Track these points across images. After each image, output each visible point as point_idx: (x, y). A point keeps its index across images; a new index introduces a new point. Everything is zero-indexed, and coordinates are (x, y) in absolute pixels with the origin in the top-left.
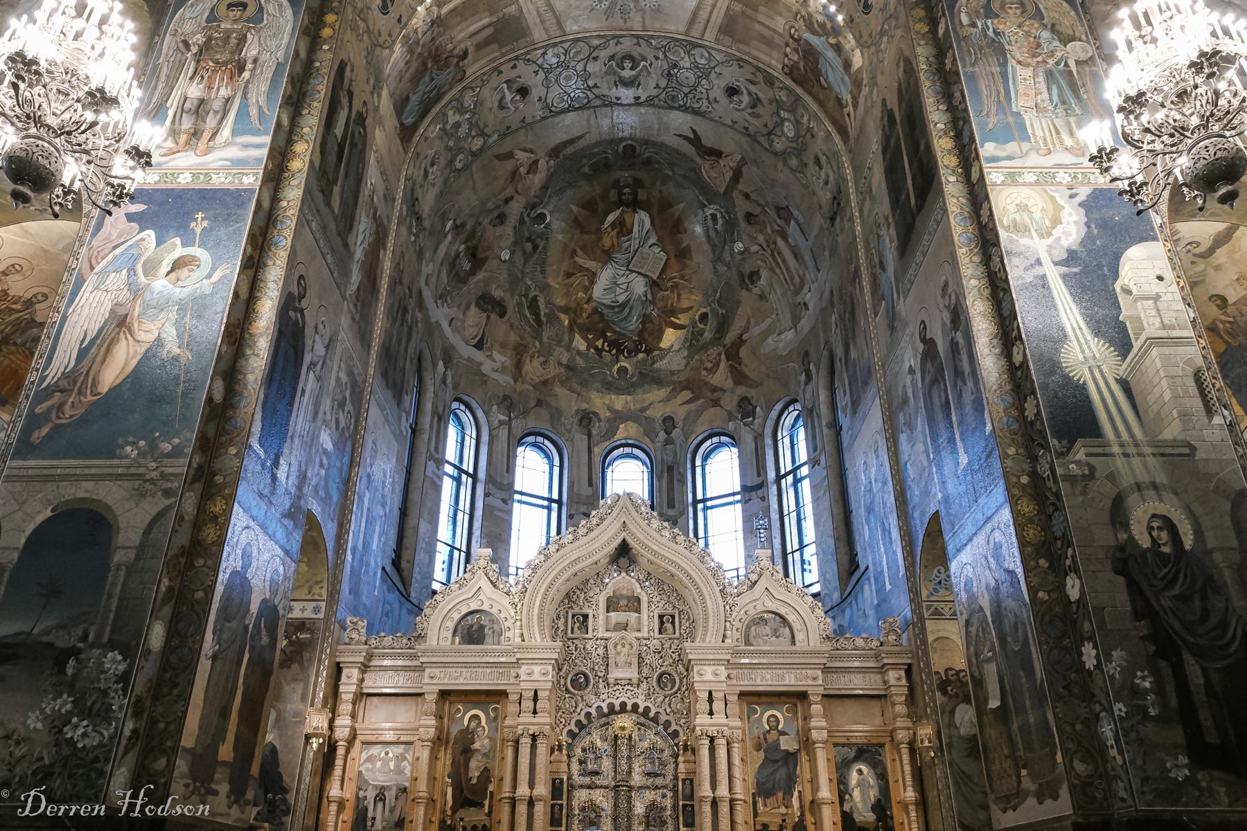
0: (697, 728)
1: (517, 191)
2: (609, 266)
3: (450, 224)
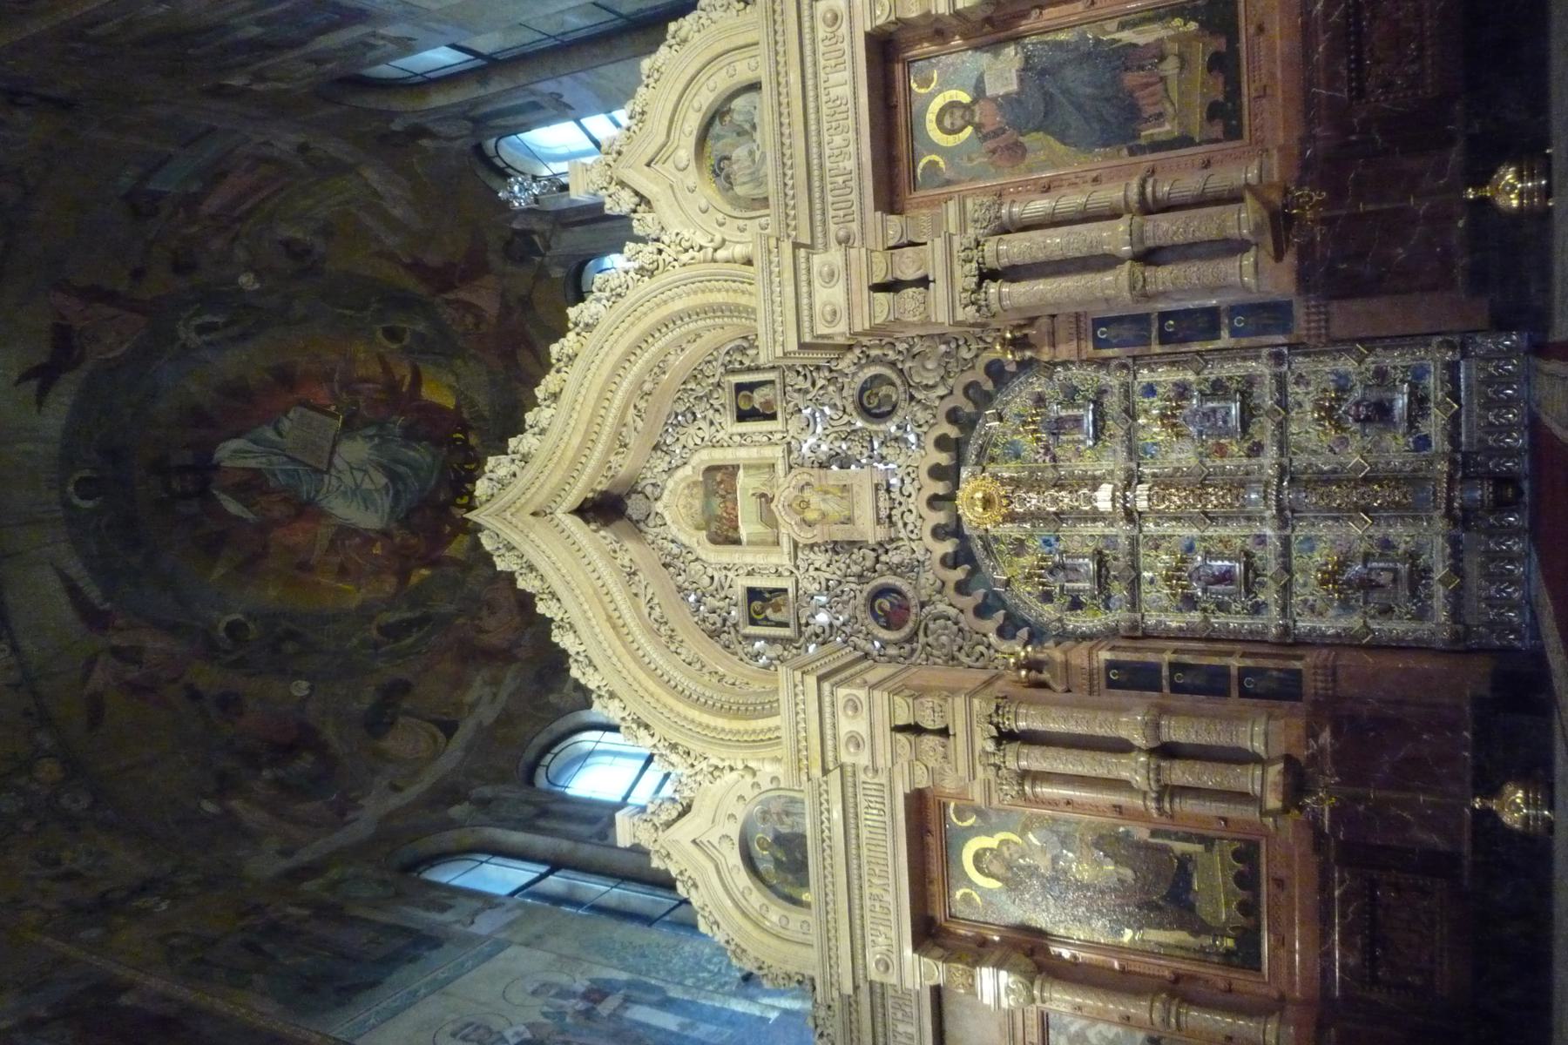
0: (960, 316)
1: (174, 681)
2: (324, 503)
3: (209, 807)
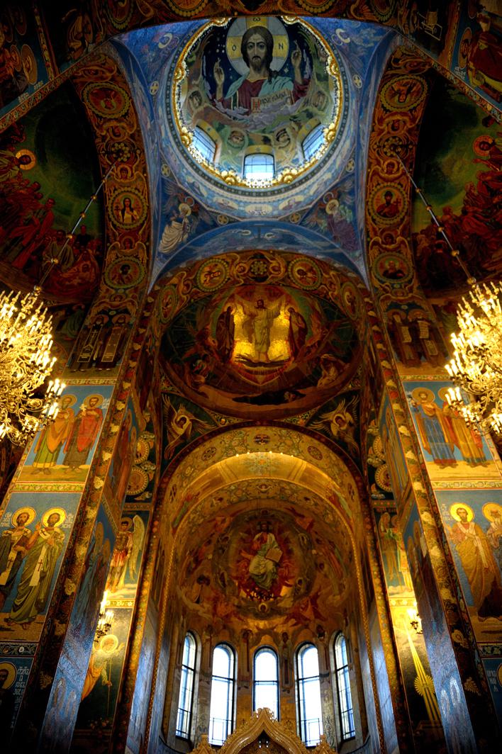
3: (188, 552)
